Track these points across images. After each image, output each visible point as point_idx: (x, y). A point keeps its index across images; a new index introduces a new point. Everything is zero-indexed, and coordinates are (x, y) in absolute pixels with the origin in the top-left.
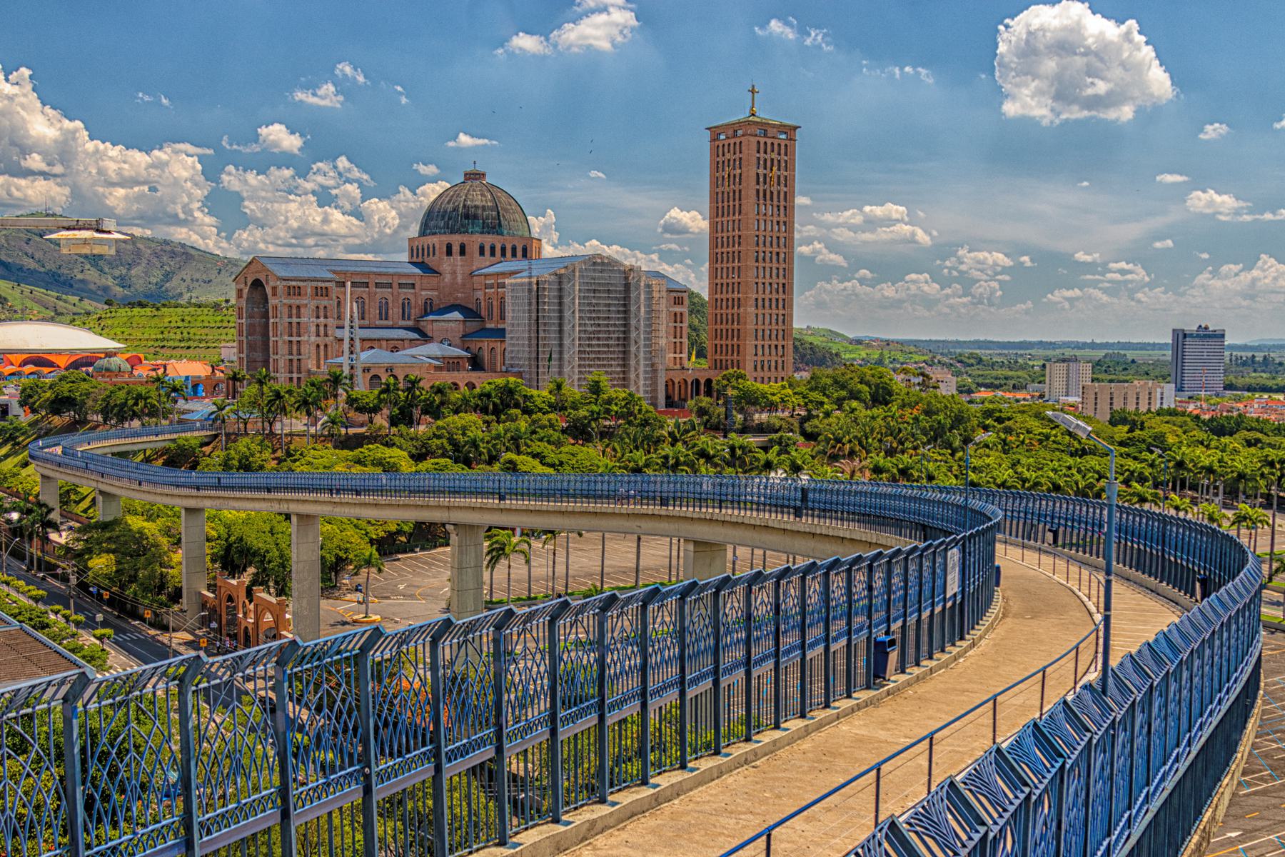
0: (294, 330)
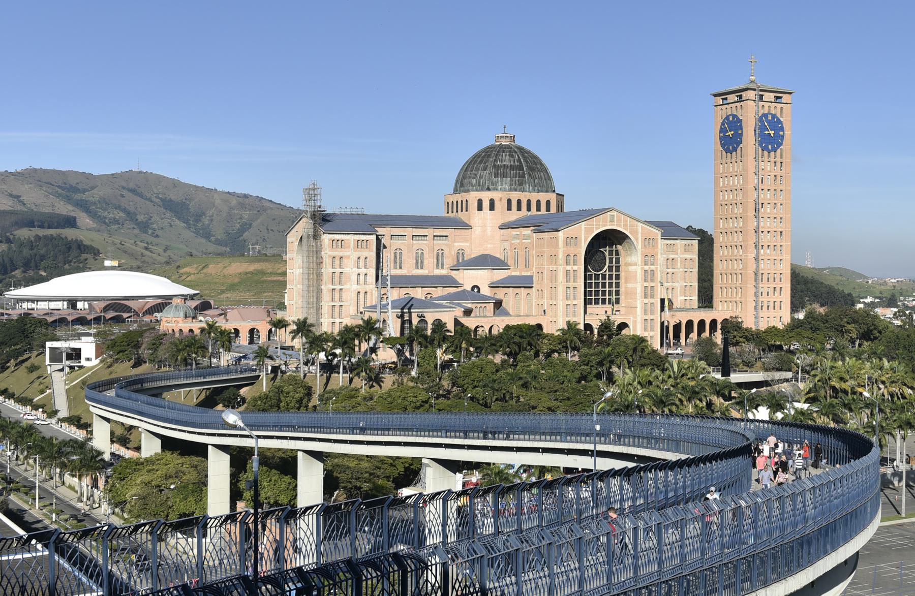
0: (337, 279)
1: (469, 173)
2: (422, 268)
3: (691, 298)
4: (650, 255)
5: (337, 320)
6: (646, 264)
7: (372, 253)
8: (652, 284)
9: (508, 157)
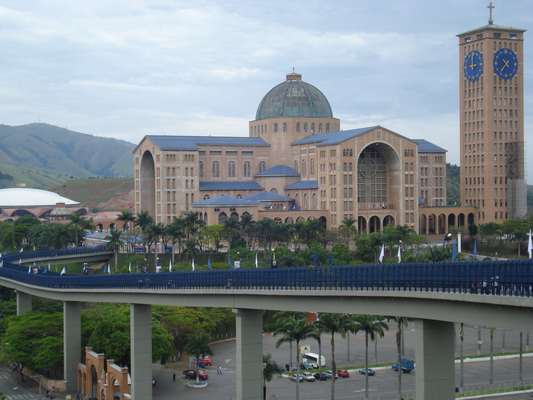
0: (171, 184)
4: (409, 163)
5: (172, 215)
6: (406, 170)
8: (412, 186)
9: (296, 91)
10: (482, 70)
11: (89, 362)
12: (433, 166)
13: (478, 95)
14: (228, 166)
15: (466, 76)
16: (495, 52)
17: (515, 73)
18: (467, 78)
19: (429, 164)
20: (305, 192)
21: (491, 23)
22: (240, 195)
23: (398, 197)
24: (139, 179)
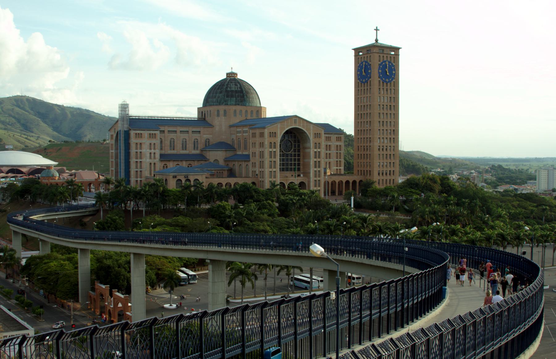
0: (139, 156)
1: (211, 95)
2: (186, 149)
3: (340, 168)
5: (139, 179)
6: (316, 148)
7: (157, 141)
8: (319, 160)
9: (234, 86)
10: (370, 76)
11: (98, 291)
12: (335, 144)
13: (367, 94)
14: (181, 142)
15: (359, 79)
16: (380, 63)
17: (394, 78)
18: (360, 80)
19: (332, 142)
20: (240, 163)
21: (377, 40)
22: (190, 164)
23: (309, 169)
24: (113, 151)
